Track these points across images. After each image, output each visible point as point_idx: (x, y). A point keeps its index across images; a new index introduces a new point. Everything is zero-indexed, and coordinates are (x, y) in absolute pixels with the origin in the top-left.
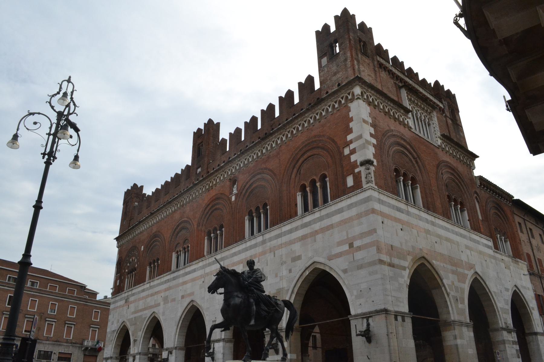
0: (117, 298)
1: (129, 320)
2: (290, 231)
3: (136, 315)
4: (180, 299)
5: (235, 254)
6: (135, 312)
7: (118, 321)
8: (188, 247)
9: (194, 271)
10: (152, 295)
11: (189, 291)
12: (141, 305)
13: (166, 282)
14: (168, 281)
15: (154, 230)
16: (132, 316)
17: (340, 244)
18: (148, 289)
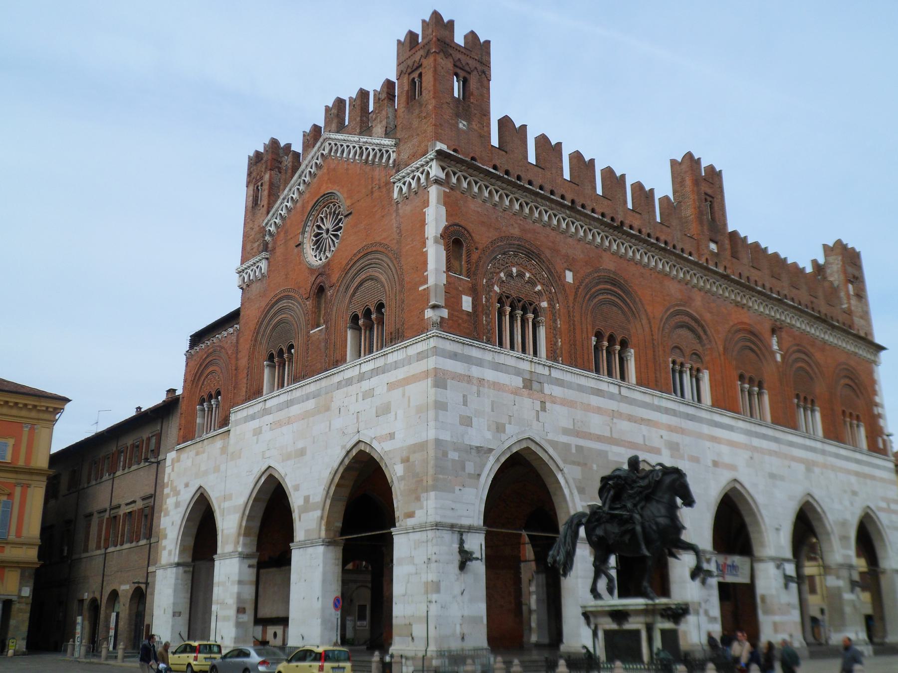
0: (475, 353)
1: (554, 444)
2: (847, 459)
3: (582, 442)
4: (710, 464)
5: (791, 444)
6: (578, 434)
7: (500, 428)
8: (698, 370)
9: (730, 428)
10: (631, 418)
11: (727, 459)
12: (596, 424)
13: (667, 411)
14: (674, 413)
15: (609, 264)
16: (564, 439)
17: (884, 499)
18: (611, 397)
